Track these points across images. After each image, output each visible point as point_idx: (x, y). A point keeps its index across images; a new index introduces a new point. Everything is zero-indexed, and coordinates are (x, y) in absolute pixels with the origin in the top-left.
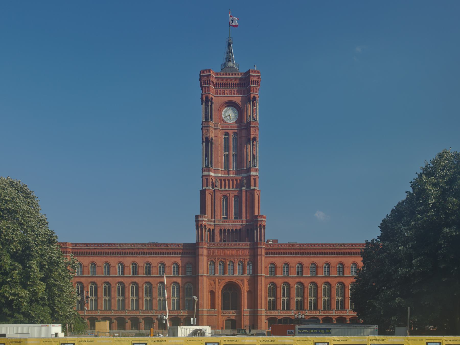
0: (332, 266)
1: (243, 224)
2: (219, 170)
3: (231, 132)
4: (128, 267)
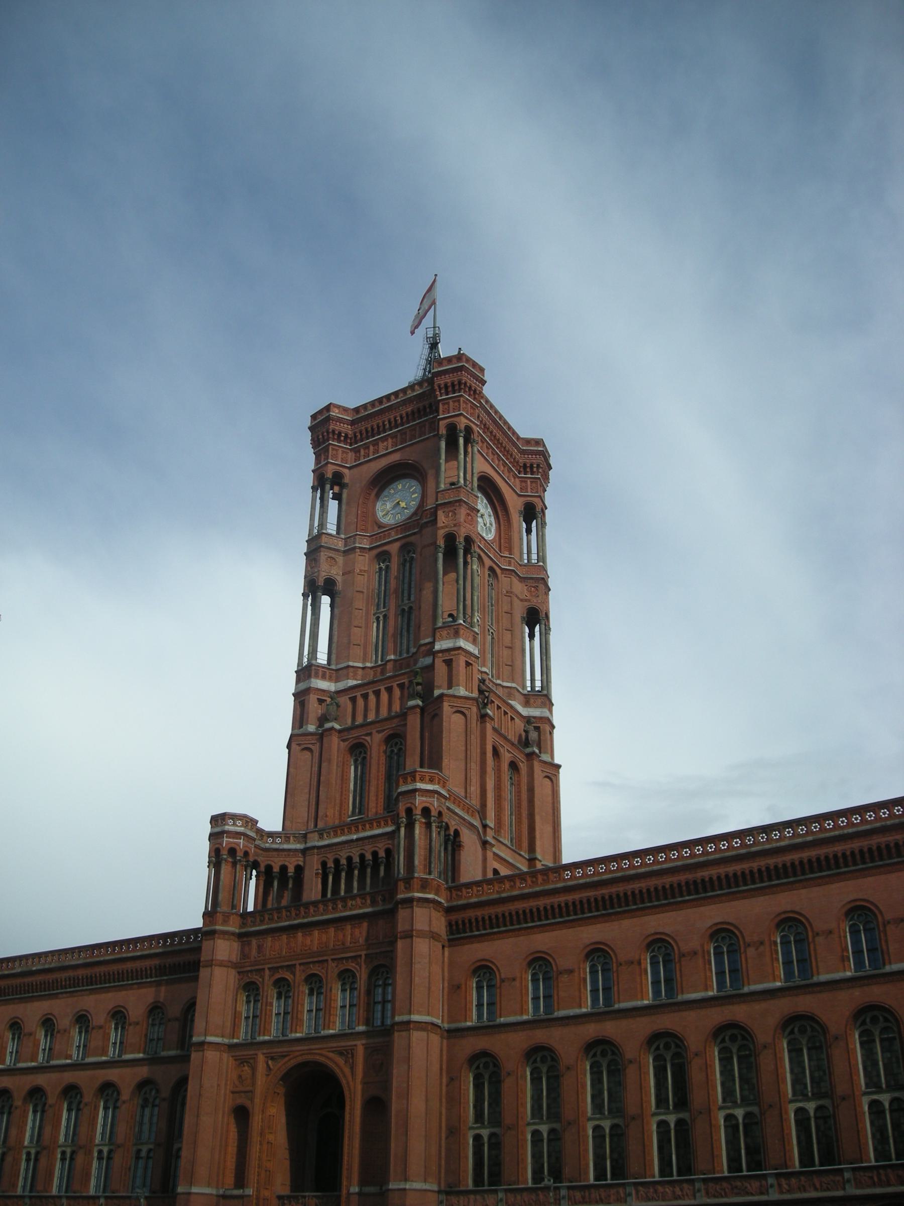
0: (748, 939)
2: (353, 667)
3: (394, 548)
4: (30, 1034)
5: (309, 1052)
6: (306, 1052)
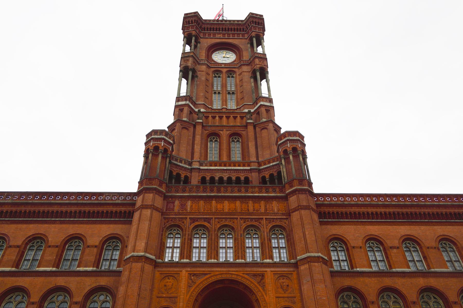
1: (252, 167)
5: (227, 272)
6: (225, 272)
